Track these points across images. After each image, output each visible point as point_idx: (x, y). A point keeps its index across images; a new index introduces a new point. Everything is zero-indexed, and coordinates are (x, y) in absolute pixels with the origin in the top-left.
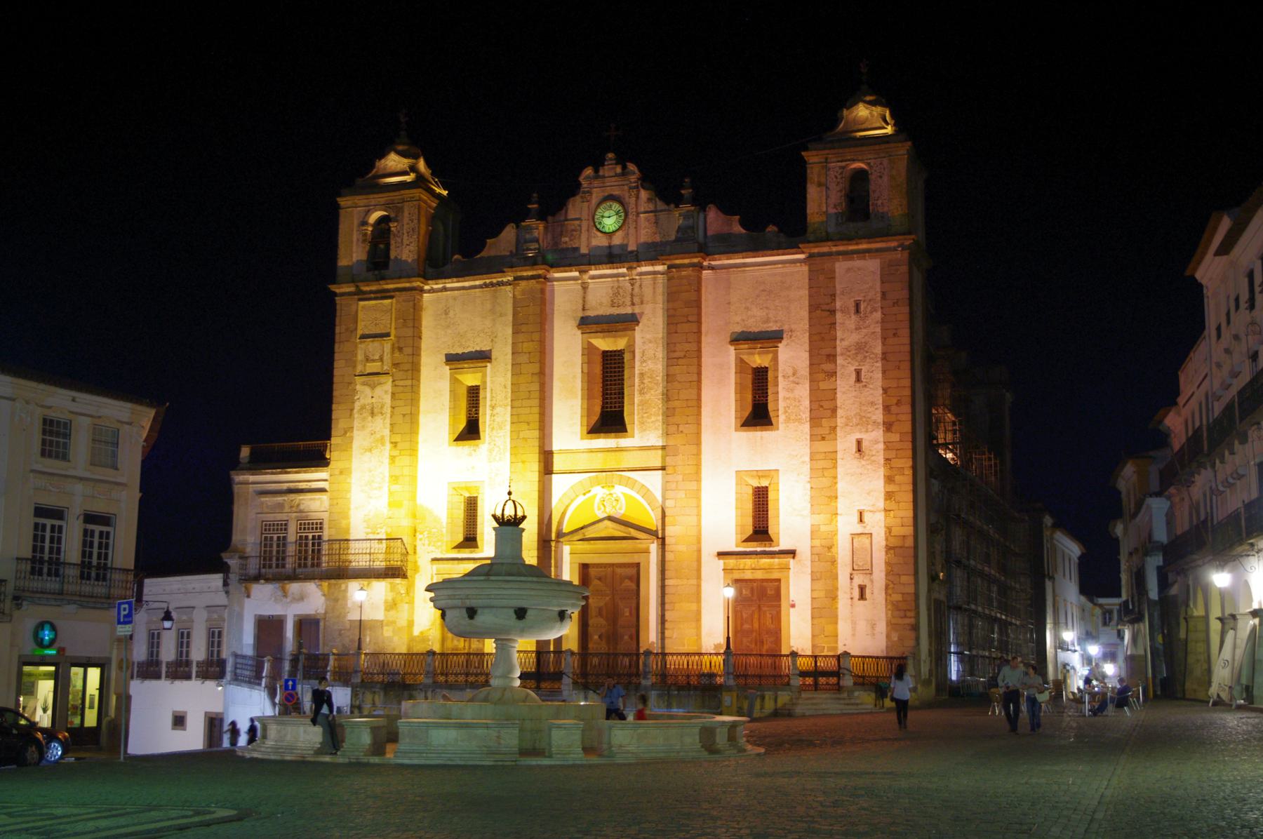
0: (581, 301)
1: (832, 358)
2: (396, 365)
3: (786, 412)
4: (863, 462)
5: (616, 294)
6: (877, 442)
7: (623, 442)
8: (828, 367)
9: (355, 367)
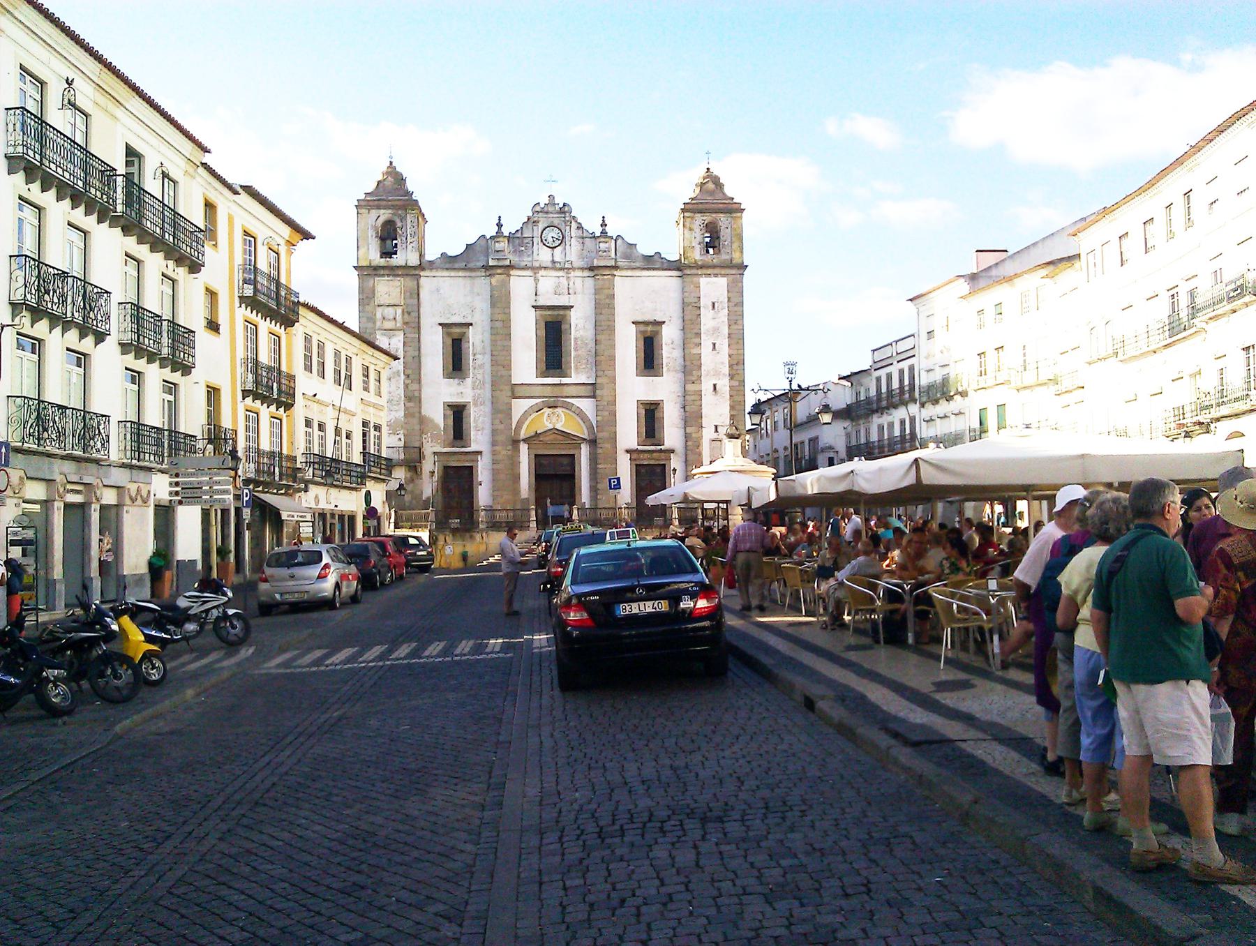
0: (534, 289)
1: (699, 335)
2: (406, 323)
3: (667, 366)
4: (717, 397)
5: (558, 286)
6: (725, 386)
7: (565, 380)
8: (697, 340)
9: (374, 323)
